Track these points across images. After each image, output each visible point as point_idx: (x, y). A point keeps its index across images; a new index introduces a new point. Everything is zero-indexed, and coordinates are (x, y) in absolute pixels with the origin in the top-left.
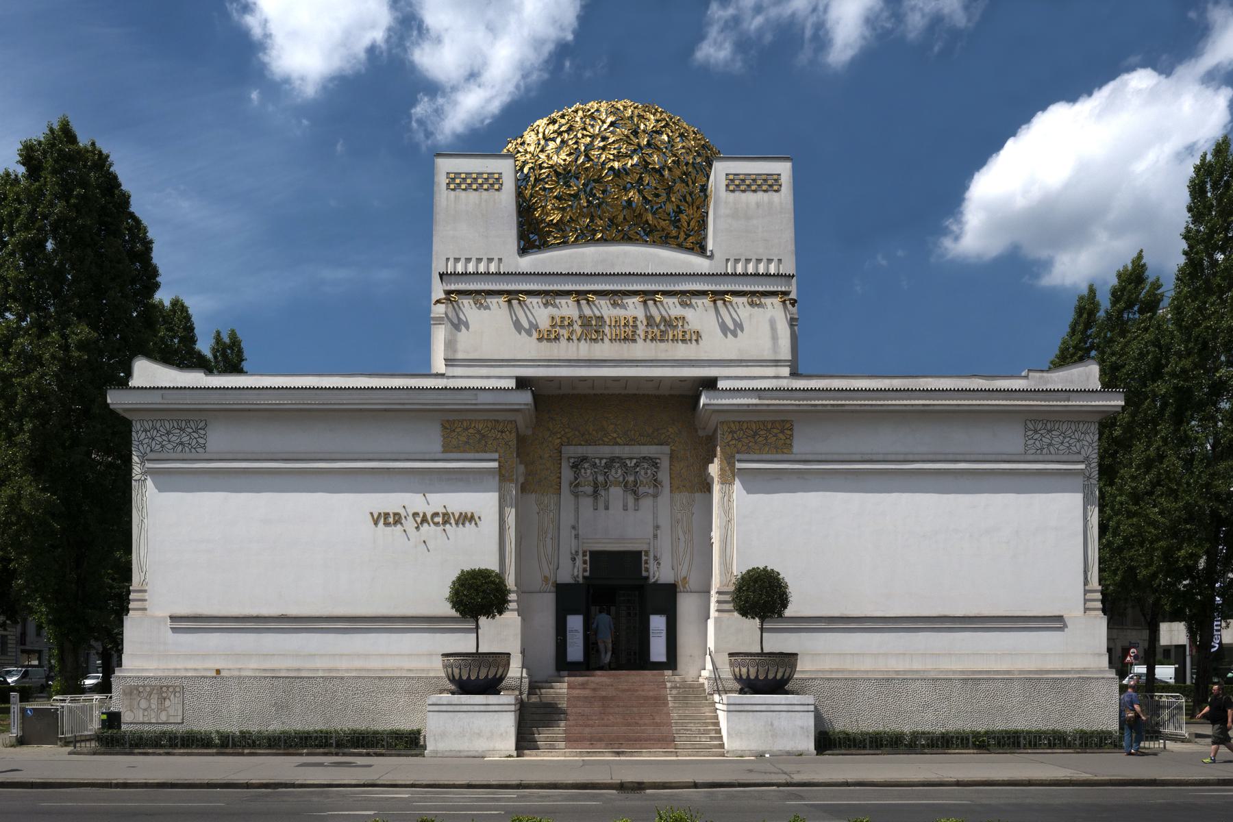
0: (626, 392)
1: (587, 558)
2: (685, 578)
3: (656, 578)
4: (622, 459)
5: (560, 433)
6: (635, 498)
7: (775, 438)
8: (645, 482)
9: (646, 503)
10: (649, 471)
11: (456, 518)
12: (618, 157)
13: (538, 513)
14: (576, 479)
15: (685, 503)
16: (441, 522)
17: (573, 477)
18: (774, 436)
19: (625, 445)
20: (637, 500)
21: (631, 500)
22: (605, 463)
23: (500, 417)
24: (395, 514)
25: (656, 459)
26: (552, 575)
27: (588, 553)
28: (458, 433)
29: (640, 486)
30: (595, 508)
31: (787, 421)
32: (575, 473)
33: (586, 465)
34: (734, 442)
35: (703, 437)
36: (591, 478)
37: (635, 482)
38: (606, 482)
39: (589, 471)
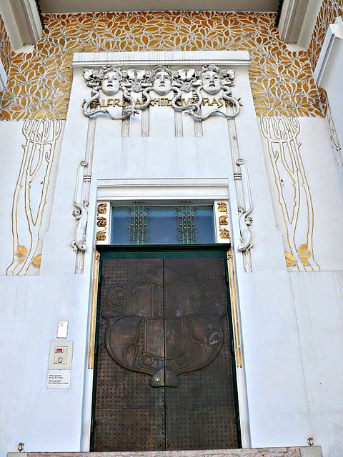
1: (107, 215)
2: (305, 247)
3: (246, 244)
6: (195, 121)
8: (211, 102)
9: (216, 127)
13: (24, 147)
14: (93, 94)
15: (282, 128)
21: (187, 121)
22: (144, 77)
27: (108, 208)
33: (111, 75)
35: (294, 53)
36: (119, 96)
37: (195, 99)
39: (115, 83)
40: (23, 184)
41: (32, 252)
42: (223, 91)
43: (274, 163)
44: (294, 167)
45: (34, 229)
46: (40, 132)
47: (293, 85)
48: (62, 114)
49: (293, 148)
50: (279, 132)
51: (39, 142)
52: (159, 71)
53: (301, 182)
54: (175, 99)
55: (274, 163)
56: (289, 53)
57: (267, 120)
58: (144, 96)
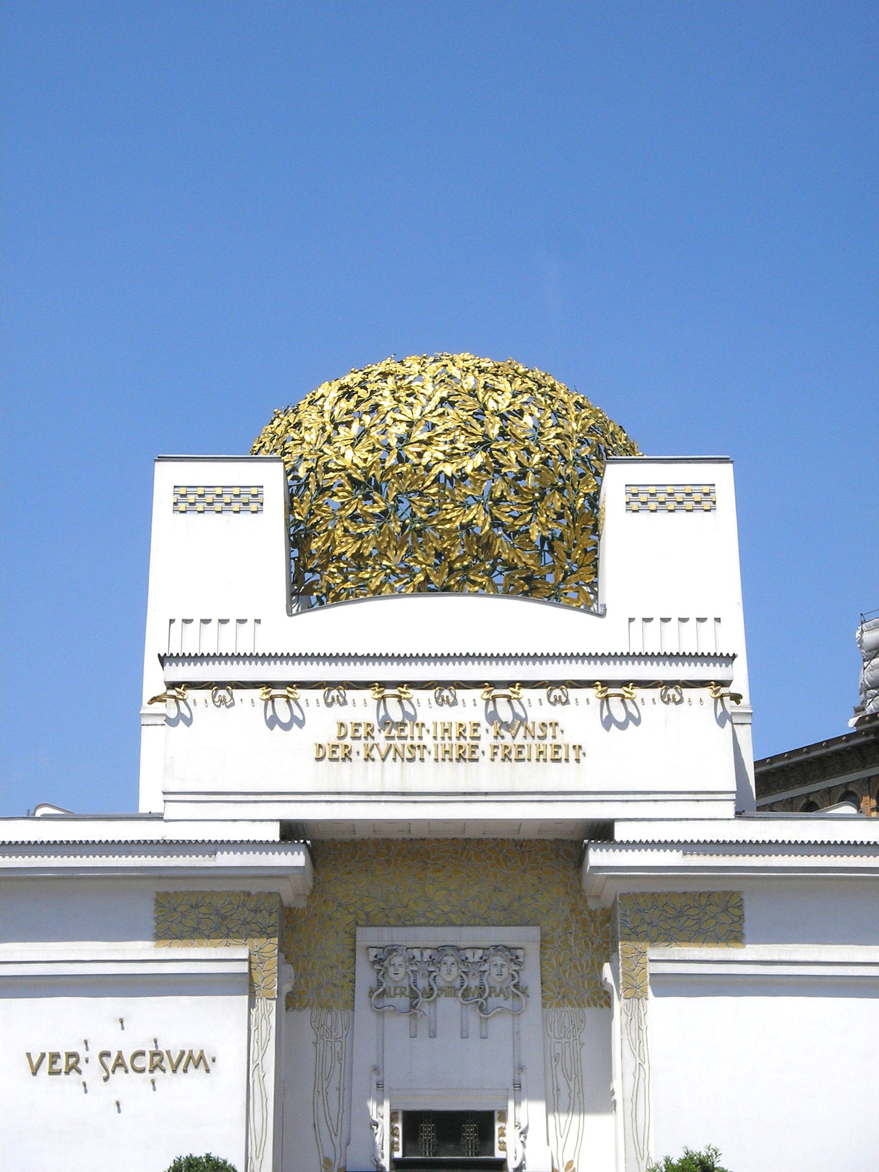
0: (466, 836)
1: (399, 1125)
4: (459, 949)
5: (353, 904)
6: (481, 1017)
7: (715, 922)
9: (500, 1025)
10: (505, 970)
11: (175, 1060)
12: (450, 457)
14: (380, 984)
15: (567, 1025)
16: (148, 1069)
17: (374, 984)
18: (712, 918)
19: (462, 925)
20: (484, 1021)
21: (473, 1018)
22: (430, 957)
23: (254, 887)
24: (70, 1055)
25: (517, 949)
26: (338, 1155)
27: (400, 1116)
28: (182, 913)
29: (490, 996)
30: (413, 1034)
31: (733, 893)
32: (378, 973)
34: (644, 927)
35: (596, 911)
37: (482, 988)
38: (432, 989)
40: (320, 1090)
41: (337, 1165)
42: (510, 978)
43: (554, 1067)
44: (573, 1073)
45: (336, 1140)
46: (329, 1024)
47: (587, 963)
48: (350, 1004)
49: (575, 1049)
50: (563, 1029)
51: (329, 1039)
52: (445, 955)
53: (577, 1090)
54: (461, 991)
55: (554, 1067)
56: (590, 912)
57: (553, 1013)
58: (430, 985)
